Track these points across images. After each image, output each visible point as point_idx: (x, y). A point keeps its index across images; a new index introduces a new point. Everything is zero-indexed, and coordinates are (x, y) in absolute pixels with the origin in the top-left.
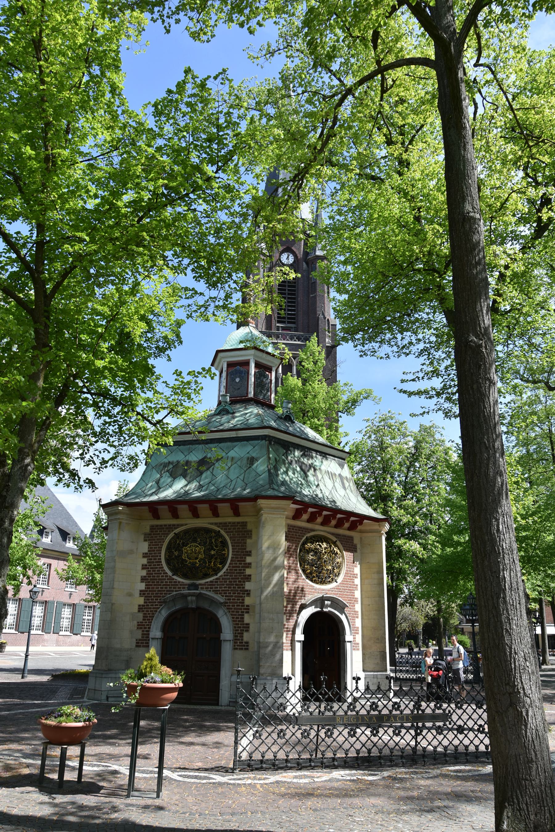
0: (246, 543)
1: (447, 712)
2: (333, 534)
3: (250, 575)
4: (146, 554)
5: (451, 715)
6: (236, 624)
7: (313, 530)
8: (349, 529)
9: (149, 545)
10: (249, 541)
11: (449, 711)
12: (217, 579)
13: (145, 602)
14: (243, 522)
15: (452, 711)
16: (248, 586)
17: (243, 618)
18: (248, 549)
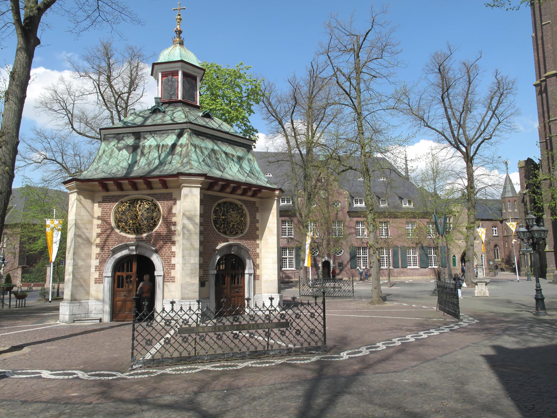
1: (289, 321)
2: (239, 200)
5: (292, 323)
7: (224, 198)
8: (253, 196)
11: (290, 320)
15: (292, 321)
17: (171, 260)
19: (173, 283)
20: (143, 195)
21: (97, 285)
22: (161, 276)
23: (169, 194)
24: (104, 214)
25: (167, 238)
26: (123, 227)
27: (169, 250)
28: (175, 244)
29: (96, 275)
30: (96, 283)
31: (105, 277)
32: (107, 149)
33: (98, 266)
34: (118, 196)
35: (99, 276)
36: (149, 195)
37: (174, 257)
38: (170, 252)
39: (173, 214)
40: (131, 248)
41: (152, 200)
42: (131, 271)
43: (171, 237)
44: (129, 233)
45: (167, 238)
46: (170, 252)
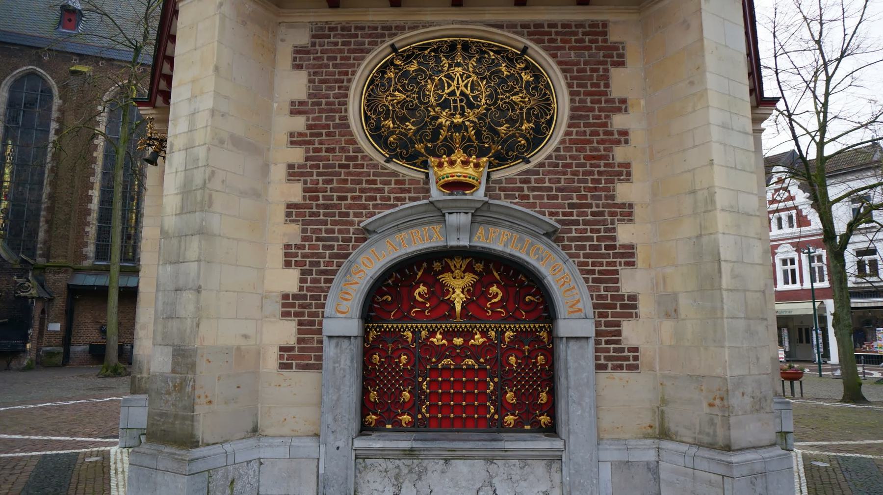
4: (301, 103)
9: (310, 81)
12: (527, 172)
13: (305, 239)
14: (593, 25)
16: (624, 192)
18: (616, 91)
19: (624, 374)
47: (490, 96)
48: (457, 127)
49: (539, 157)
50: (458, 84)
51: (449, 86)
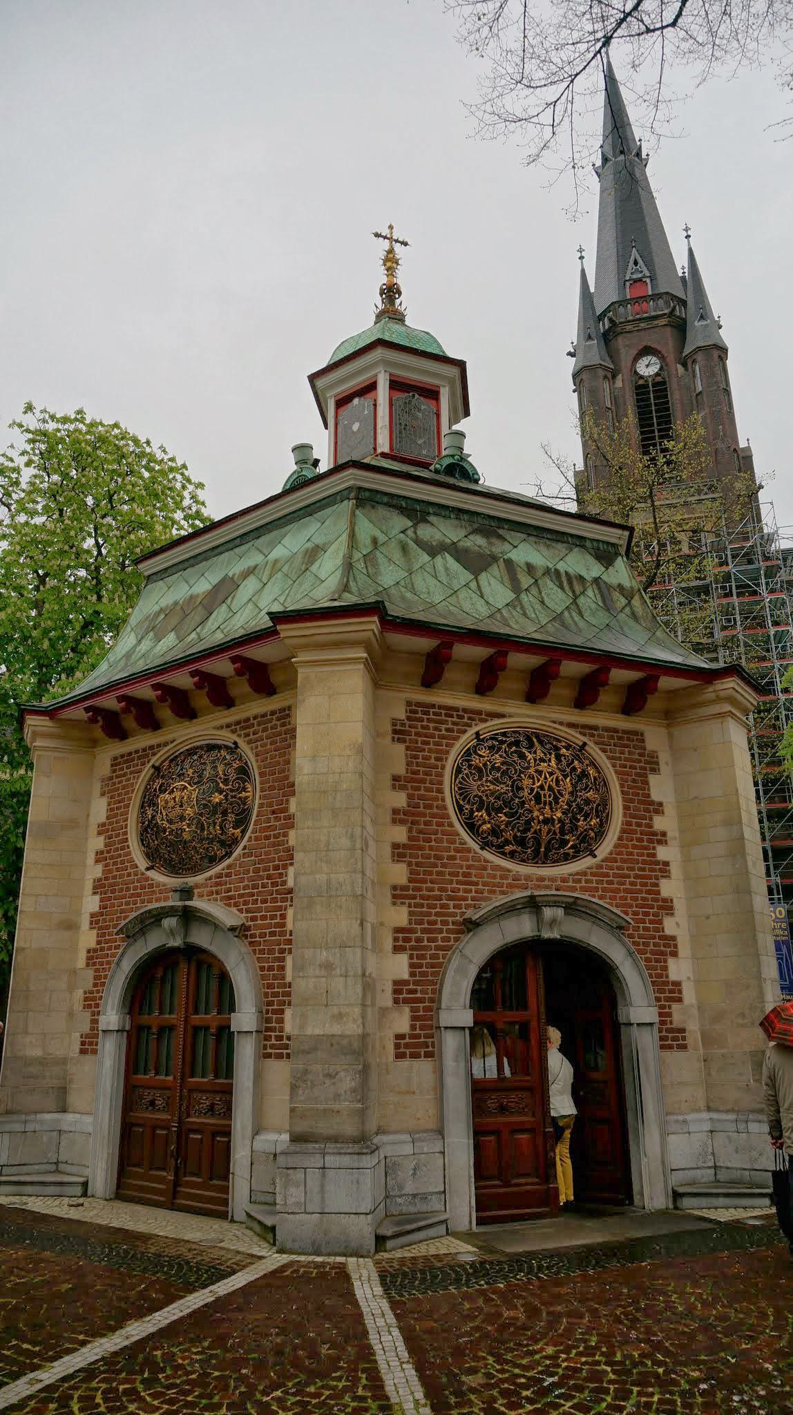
0: (647, 783)
3: (666, 864)
6: (270, 986)
10: (652, 779)
20: (554, 722)
21: (406, 1063)
22: (651, 1024)
23: (636, 733)
24: (417, 772)
25: (645, 885)
26: (495, 832)
27: (656, 930)
28: (671, 908)
29: (402, 1022)
30: (399, 1056)
31: (446, 1028)
32: (382, 538)
33: (406, 983)
34: (465, 710)
35: (413, 1027)
36: (571, 725)
37: (674, 954)
38: (660, 938)
39: (652, 803)
40: (548, 912)
41: (585, 744)
42: (524, 1005)
43: (657, 885)
44: (512, 855)
45: (645, 885)
46: (660, 938)
47: (571, 793)
48: (546, 821)
49: (605, 848)
50: (546, 778)
51: (539, 780)
